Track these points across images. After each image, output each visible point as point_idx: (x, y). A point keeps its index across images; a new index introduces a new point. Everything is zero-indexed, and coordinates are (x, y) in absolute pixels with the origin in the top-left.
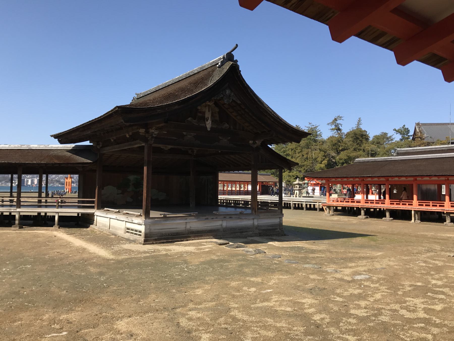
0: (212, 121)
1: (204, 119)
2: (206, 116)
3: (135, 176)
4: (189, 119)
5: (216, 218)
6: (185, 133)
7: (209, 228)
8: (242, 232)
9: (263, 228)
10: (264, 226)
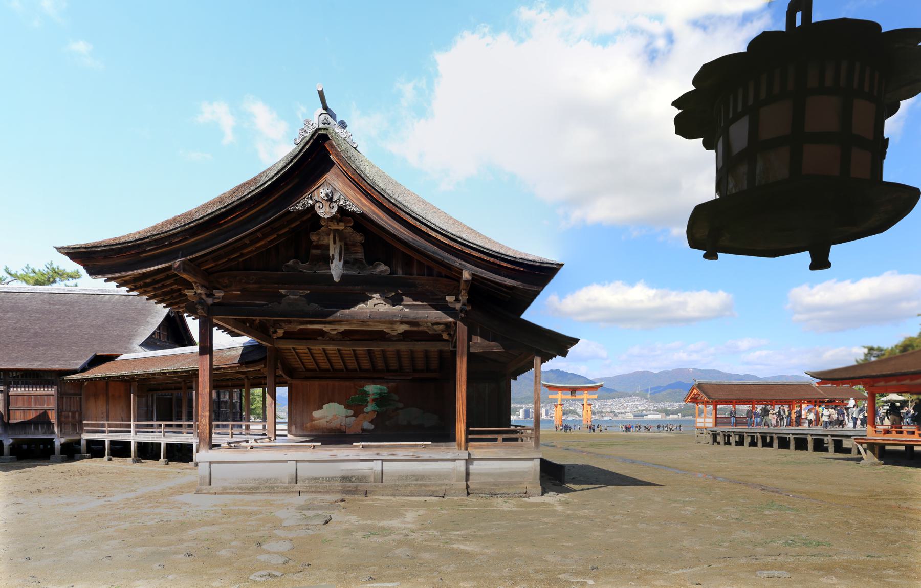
0: (345, 263)
1: (327, 260)
3: (378, 386)
4: (291, 262)
6: (283, 291)
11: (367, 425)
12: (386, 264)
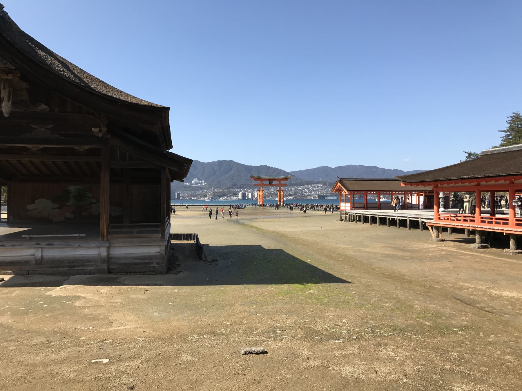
0: (14, 103)
2: (2, 95)
3: (78, 187)
5: (21, 245)
7: (9, 259)
8: (74, 267)
9: (124, 261)
10: (125, 258)
11: (69, 215)
12: (45, 105)
